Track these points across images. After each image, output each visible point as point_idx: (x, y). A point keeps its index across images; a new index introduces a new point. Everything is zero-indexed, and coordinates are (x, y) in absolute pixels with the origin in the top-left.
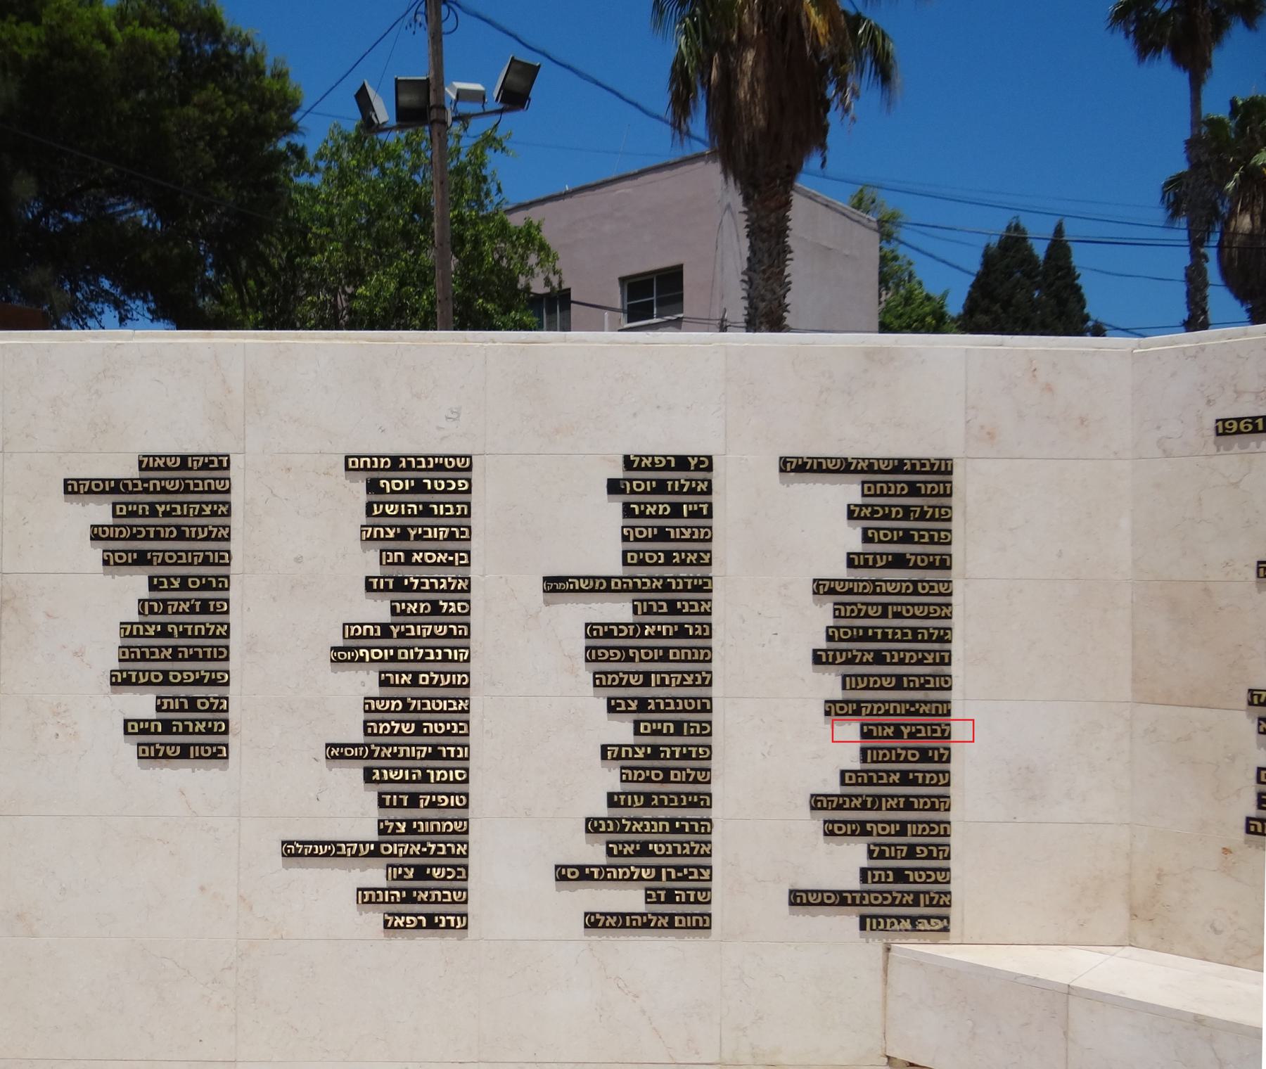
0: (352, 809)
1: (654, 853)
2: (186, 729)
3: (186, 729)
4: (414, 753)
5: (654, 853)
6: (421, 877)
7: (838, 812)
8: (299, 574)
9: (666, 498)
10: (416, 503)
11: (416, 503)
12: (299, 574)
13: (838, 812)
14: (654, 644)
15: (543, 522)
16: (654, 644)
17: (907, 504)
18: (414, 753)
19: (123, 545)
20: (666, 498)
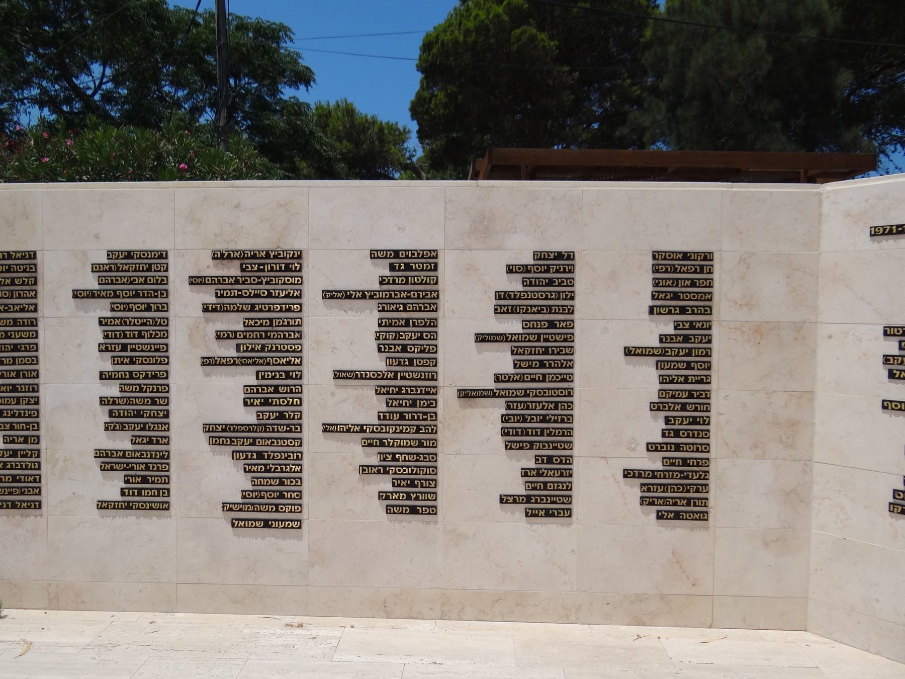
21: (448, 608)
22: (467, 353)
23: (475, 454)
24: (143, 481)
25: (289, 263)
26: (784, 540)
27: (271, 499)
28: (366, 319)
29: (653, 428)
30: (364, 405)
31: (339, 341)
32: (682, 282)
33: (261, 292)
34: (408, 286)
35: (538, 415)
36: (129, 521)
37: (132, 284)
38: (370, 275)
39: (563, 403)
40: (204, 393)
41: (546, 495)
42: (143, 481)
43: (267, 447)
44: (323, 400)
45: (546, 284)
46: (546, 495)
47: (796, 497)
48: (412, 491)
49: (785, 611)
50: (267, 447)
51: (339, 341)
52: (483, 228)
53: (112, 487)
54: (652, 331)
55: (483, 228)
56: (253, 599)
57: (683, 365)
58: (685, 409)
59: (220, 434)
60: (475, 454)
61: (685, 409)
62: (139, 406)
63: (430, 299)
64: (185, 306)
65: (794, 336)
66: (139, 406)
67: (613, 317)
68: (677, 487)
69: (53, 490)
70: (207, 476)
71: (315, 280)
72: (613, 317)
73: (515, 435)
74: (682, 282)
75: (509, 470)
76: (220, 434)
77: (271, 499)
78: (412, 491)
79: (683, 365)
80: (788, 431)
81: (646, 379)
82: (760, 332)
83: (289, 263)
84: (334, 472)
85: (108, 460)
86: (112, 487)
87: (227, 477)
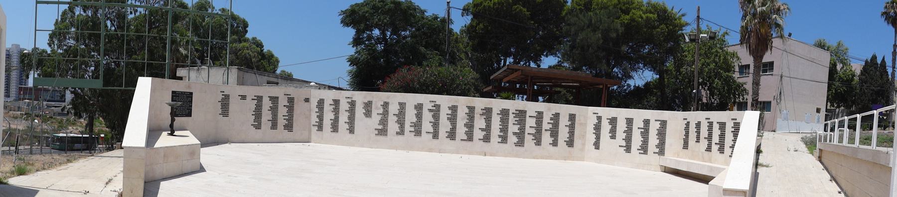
0: (624, 144)
1: (644, 149)
2: (613, 137)
3: (613, 137)
4: (628, 139)
5: (644, 149)
6: (628, 149)
7: (657, 146)
8: (621, 126)
9: (647, 122)
10: (630, 122)
11: (630, 122)
12: (621, 126)
13: (657, 146)
14: (645, 133)
15: (638, 124)
16: (645, 133)
17: (664, 124)
18: (628, 139)
19: (610, 123)
20: (647, 122)
21: (542, 158)
22: (546, 125)
23: (546, 138)
24: (504, 139)
25: (525, 112)
26: (582, 150)
27: (520, 143)
28: (534, 120)
29: (568, 135)
30: (533, 131)
31: (530, 122)
32: (572, 117)
33: (521, 115)
34: (540, 116)
35: (554, 133)
36: (501, 145)
37: (505, 113)
38: (535, 114)
39: (557, 132)
40: (513, 128)
41: (555, 144)
42: (504, 139)
43: (520, 136)
44: (528, 130)
45: (556, 116)
46: (555, 144)
47: (584, 144)
48: (538, 142)
49: (582, 159)
50: (520, 136)
51: (530, 122)
52: (549, 109)
53: (500, 140)
54: (568, 123)
55: (549, 109)
56: (517, 156)
57: (572, 127)
58: (572, 133)
59: (515, 134)
60: (546, 138)
61: (572, 133)
62: (504, 129)
63: (542, 118)
64: (511, 116)
65: (585, 125)
66: (504, 129)
67: (564, 122)
68: (570, 143)
69: (492, 140)
70: (513, 139)
71: (528, 115)
72: (564, 122)
73: (552, 136)
74: (572, 117)
75: (551, 140)
76: (515, 134)
77: (520, 143)
78: (538, 142)
79: (572, 127)
80: (583, 136)
81: (567, 129)
82: (581, 124)
83: (525, 112)
84: (529, 139)
85: (500, 136)
86: (500, 140)
87: (515, 139)
